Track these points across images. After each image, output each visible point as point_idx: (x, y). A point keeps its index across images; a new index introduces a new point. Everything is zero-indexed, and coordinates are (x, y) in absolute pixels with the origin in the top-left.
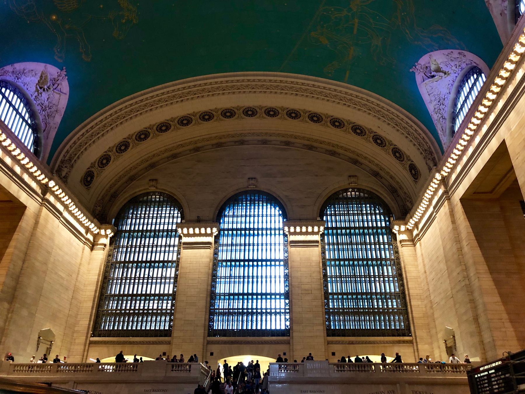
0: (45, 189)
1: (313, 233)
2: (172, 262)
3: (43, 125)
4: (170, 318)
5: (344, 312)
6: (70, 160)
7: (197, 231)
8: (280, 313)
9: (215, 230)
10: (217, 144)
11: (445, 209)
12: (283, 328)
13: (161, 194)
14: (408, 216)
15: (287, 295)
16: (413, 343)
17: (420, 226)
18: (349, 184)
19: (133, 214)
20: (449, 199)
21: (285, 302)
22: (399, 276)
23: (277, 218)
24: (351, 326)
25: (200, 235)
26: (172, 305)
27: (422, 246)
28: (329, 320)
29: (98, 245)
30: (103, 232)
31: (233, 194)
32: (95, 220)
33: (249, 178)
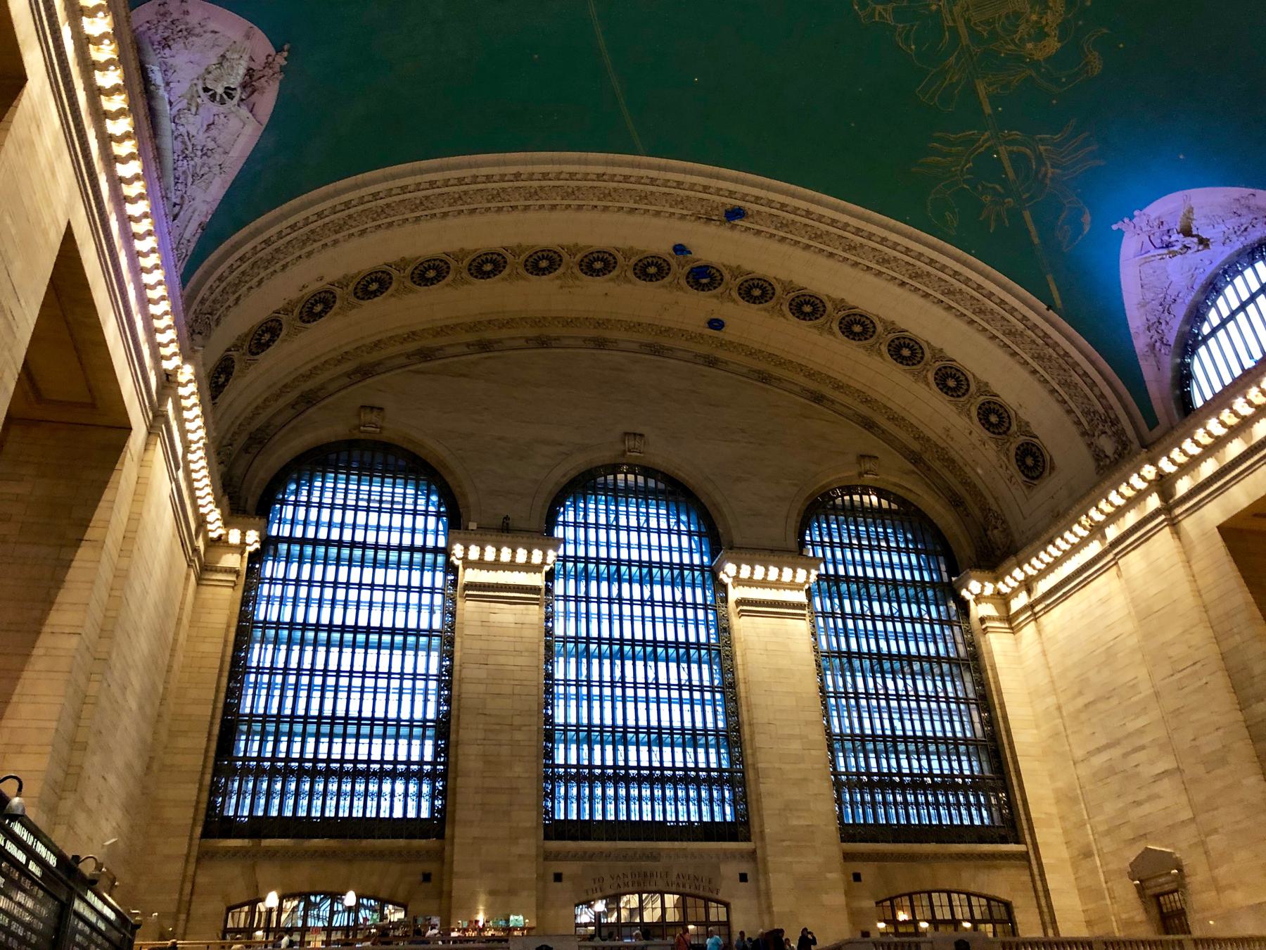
1: (793, 586)
2: (430, 633)
4: (434, 788)
8: (720, 782)
14: (1013, 560)
16: (1029, 861)
18: (860, 475)
19: (297, 492)
20: (1174, 524)
21: (729, 753)
24: (927, 817)
25: (512, 566)
30: (234, 536)
32: (225, 500)
33: (626, 434)
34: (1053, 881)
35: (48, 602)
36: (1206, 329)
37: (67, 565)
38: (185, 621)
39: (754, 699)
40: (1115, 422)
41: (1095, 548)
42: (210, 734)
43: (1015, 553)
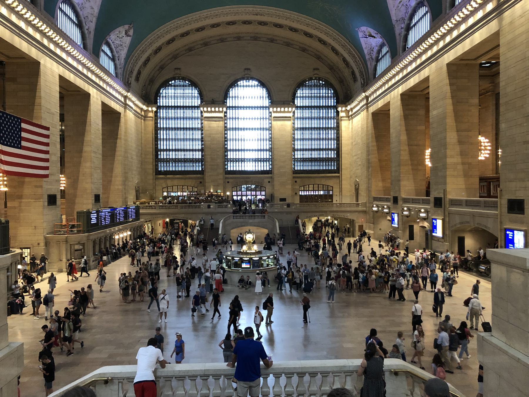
0: (126, 97)
1: (288, 112)
3: (117, 56)
5: (304, 160)
10: (220, 39)
11: (363, 114)
12: (268, 169)
13: (184, 79)
14: (348, 103)
17: (354, 111)
20: (367, 108)
22: (338, 139)
23: (264, 98)
25: (215, 112)
26: (202, 156)
28: (294, 165)
29: (147, 117)
30: (150, 109)
32: (146, 103)
33: (245, 69)
34: (343, 182)
37: (116, 143)
38: (143, 131)
41: (358, 108)
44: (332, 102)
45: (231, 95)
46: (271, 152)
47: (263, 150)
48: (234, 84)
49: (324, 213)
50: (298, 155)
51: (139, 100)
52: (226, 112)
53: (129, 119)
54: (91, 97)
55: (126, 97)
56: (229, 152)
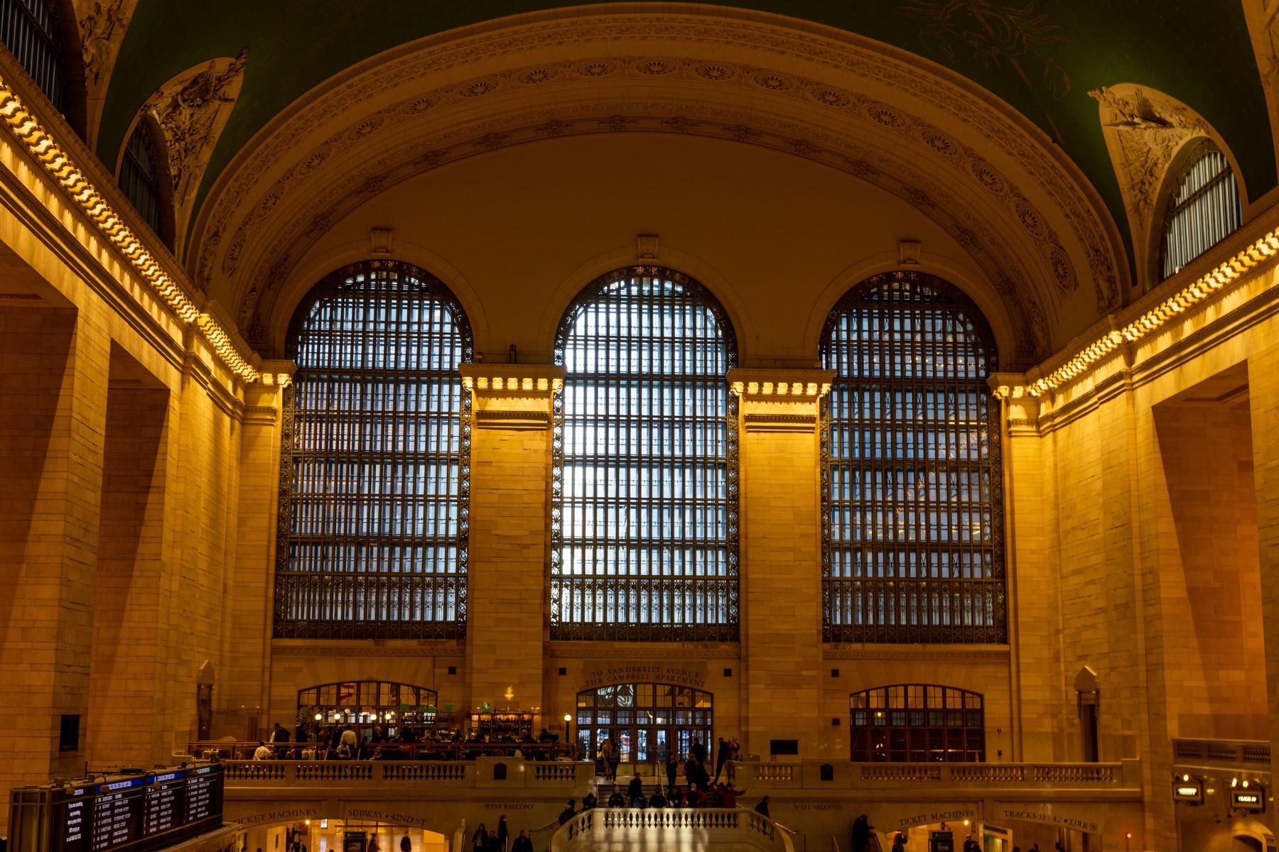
1: (804, 398)
3: (173, 172)
6: (216, 234)
7: (513, 384)
8: (715, 589)
9: (557, 383)
13: (403, 269)
14: (1035, 370)
15: (733, 546)
20: (1132, 388)
21: (727, 562)
22: (997, 506)
25: (520, 393)
26: (459, 564)
27: (1061, 444)
30: (268, 379)
31: (595, 276)
32: (256, 356)
35: (136, 537)
36: (1179, 201)
37: (142, 507)
39: (750, 515)
40: (1109, 268)
41: (1088, 385)
42: (268, 556)
43: (1038, 362)
44: (968, 366)
45: (580, 331)
46: (737, 552)
47: (705, 546)
48: (591, 293)
49: (971, 807)
50: (843, 567)
51: (233, 344)
52: (561, 396)
53: (194, 415)
54: (80, 321)
55: (190, 331)
56: (566, 552)
